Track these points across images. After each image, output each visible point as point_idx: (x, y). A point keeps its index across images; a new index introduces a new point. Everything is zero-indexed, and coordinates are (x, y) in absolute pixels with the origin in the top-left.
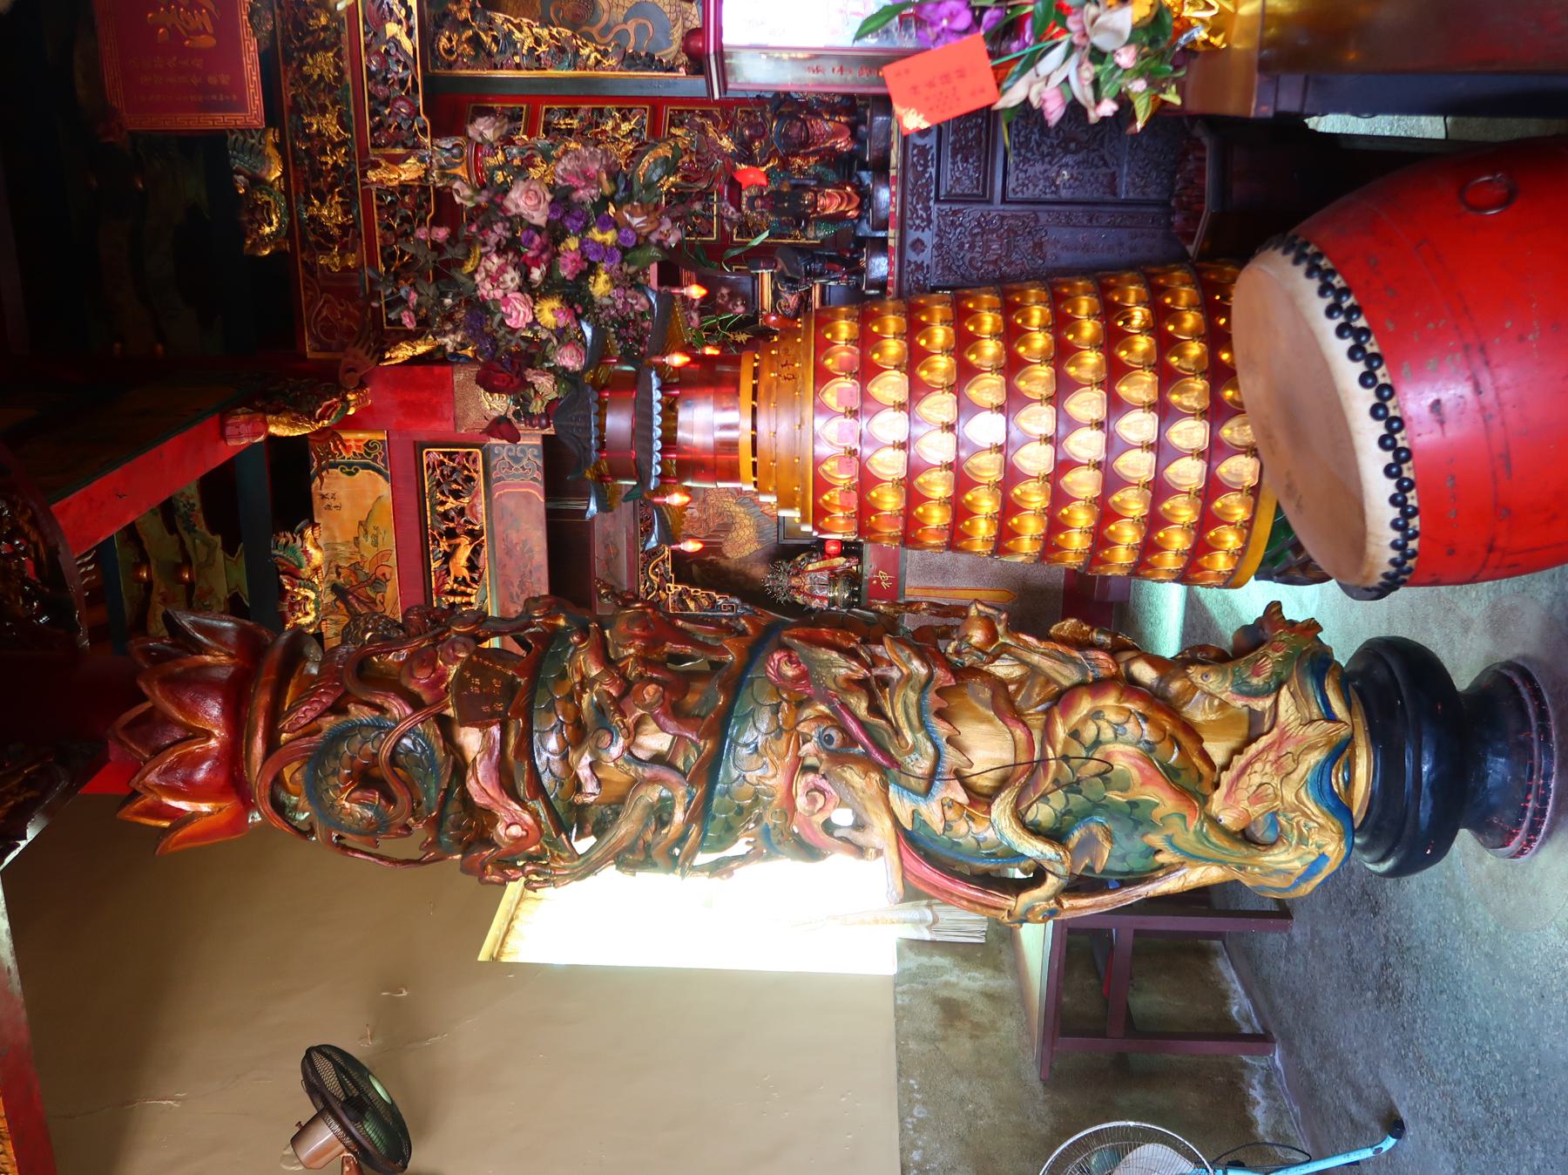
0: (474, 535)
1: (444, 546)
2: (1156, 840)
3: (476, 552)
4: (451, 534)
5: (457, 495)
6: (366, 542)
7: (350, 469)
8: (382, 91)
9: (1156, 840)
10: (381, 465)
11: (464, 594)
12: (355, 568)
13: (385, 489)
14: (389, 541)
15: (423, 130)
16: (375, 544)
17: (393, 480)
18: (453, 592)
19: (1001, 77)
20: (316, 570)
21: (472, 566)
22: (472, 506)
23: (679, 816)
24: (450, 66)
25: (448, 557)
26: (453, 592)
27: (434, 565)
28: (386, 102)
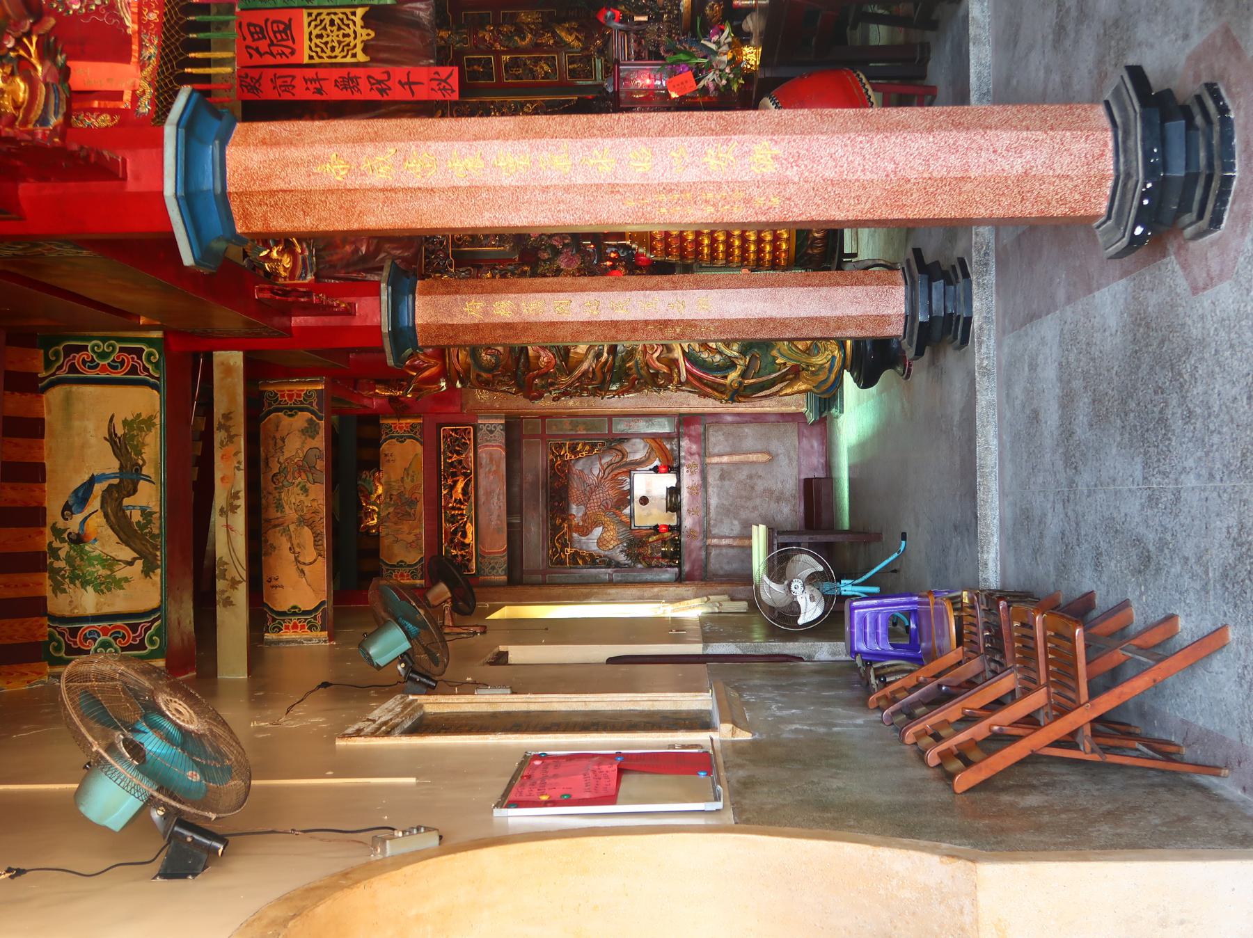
0: (466, 475)
1: (450, 482)
2: (775, 353)
3: (467, 485)
4: (454, 475)
5: (459, 453)
6: (408, 480)
7: (401, 440)
8: (431, 247)
9: (775, 353)
10: (418, 436)
11: (459, 509)
12: (401, 494)
13: (419, 449)
14: (420, 479)
15: (451, 266)
16: (412, 481)
17: (423, 444)
18: (453, 508)
19: (698, 82)
20: (379, 497)
21: (465, 491)
22: (467, 458)
23: (605, 355)
24: (459, 246)
25: (452, 487)
26: (453, 508)
27: (444, 492)
28: (433, 252)
